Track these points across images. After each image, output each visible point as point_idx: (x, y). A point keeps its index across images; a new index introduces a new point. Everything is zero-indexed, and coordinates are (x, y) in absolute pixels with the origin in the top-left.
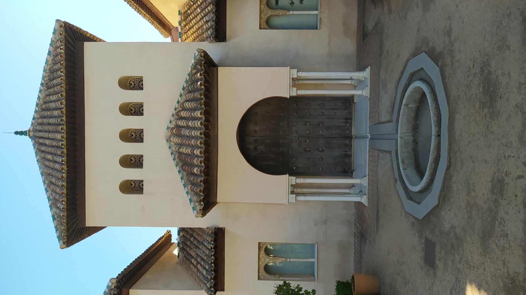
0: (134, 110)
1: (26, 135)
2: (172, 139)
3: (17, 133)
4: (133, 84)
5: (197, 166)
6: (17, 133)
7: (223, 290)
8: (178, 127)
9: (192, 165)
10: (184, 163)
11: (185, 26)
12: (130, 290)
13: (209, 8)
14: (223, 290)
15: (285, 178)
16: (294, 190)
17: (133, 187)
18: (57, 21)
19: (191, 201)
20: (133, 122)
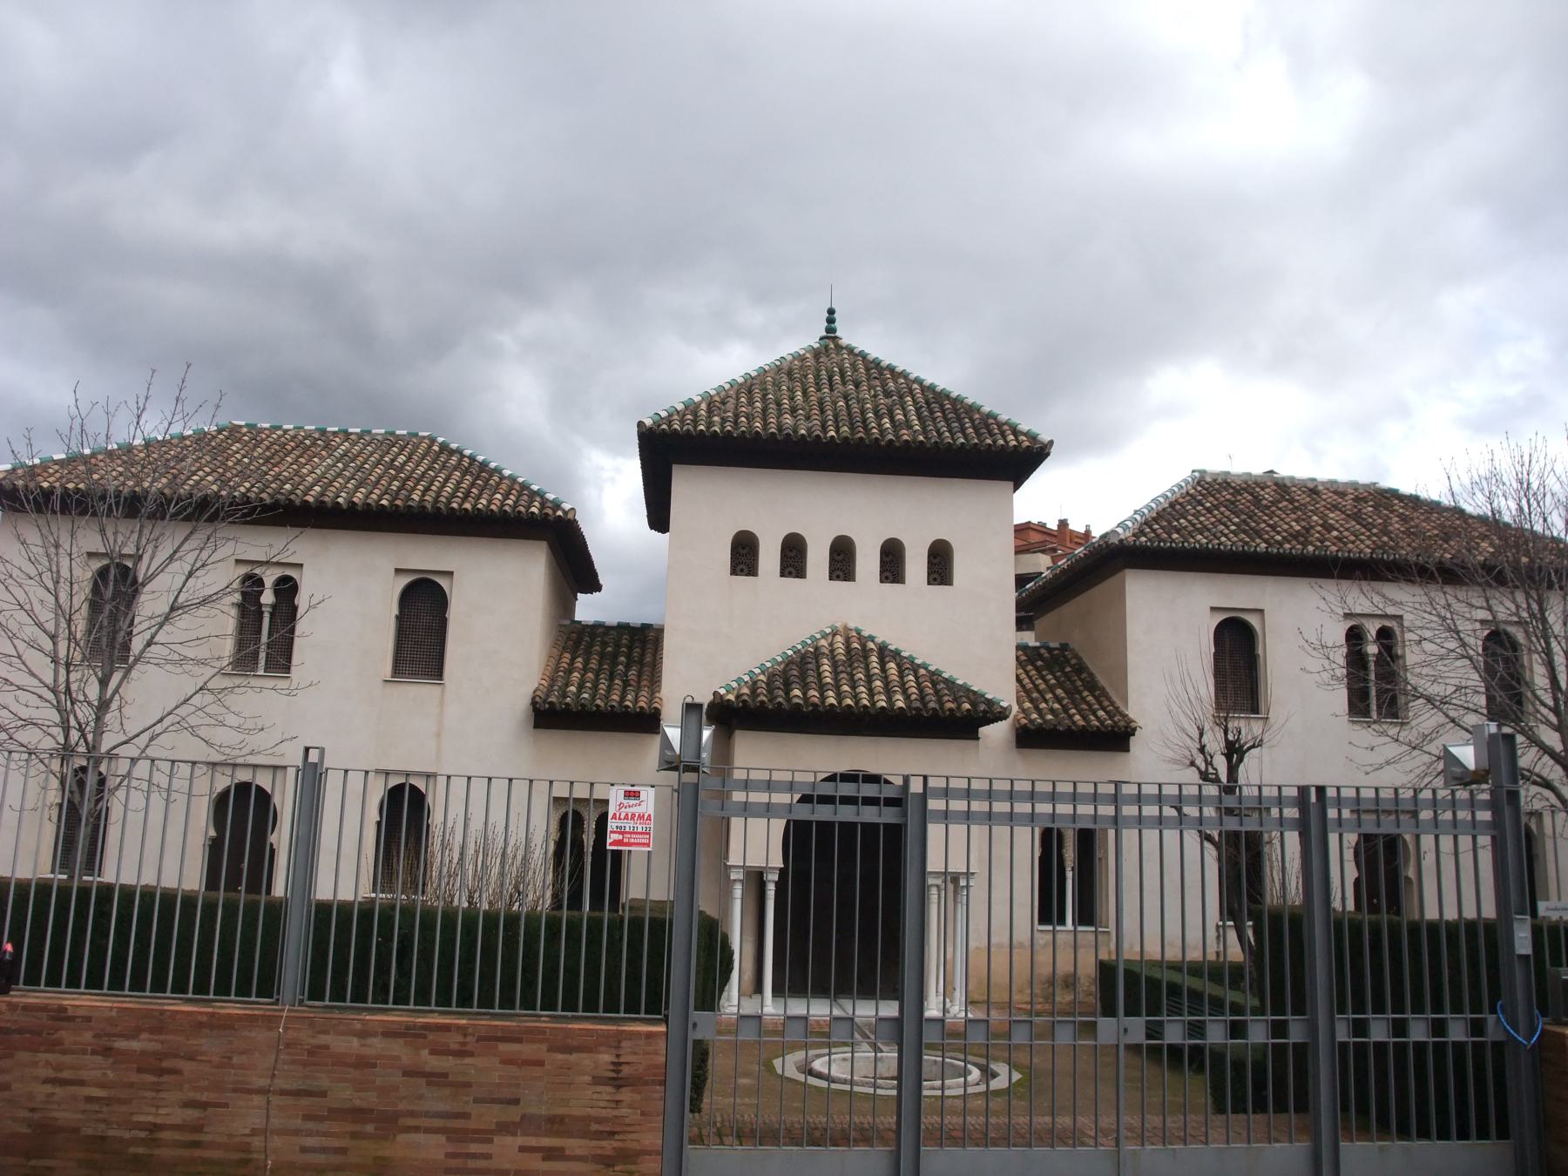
0: (892, 562)
1: (828, 330)
2: (838, 638)
3: (831, 312)
4: (940, 564)
5: (805, 694)
6: (831, 312)
7: (537, 726)
8: (866, 653)
9: (805, 688)
10: (802, 664)
11: (1041, 657)
12: (544, 544)
13: (1077, 717)
14: (537, 726)
15: (777, 861)
16: (756, 879)
17: (744, 554)
18: (1051, 442)
19: (738, 680)
20: (868, 561)
